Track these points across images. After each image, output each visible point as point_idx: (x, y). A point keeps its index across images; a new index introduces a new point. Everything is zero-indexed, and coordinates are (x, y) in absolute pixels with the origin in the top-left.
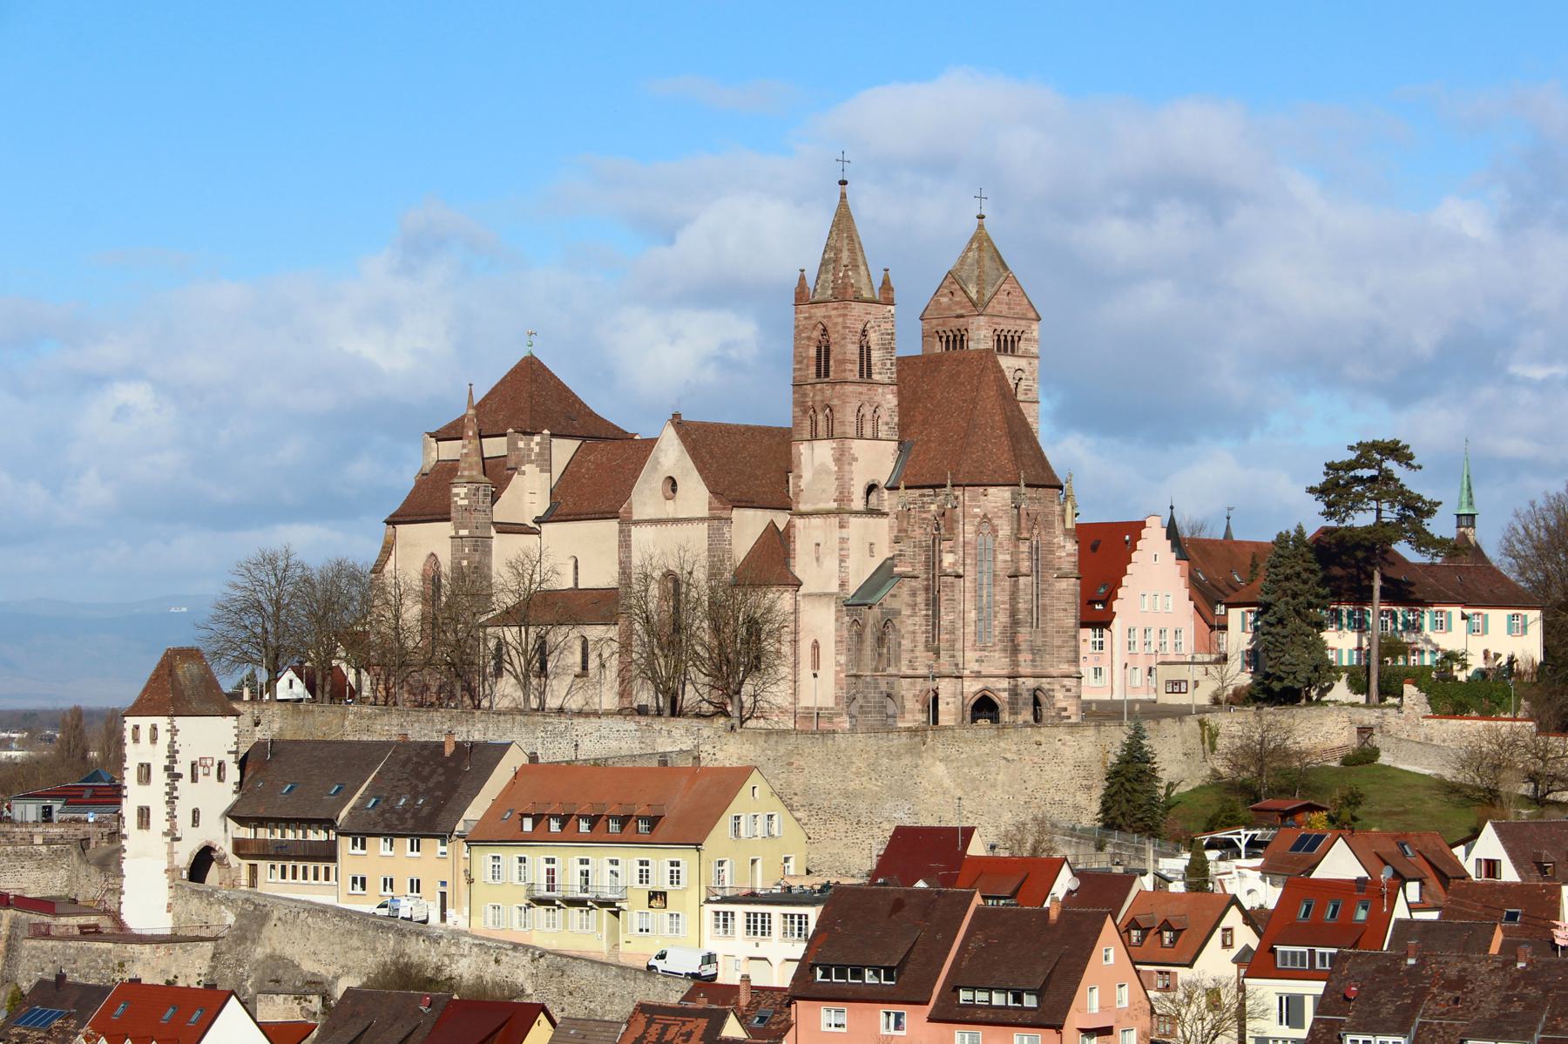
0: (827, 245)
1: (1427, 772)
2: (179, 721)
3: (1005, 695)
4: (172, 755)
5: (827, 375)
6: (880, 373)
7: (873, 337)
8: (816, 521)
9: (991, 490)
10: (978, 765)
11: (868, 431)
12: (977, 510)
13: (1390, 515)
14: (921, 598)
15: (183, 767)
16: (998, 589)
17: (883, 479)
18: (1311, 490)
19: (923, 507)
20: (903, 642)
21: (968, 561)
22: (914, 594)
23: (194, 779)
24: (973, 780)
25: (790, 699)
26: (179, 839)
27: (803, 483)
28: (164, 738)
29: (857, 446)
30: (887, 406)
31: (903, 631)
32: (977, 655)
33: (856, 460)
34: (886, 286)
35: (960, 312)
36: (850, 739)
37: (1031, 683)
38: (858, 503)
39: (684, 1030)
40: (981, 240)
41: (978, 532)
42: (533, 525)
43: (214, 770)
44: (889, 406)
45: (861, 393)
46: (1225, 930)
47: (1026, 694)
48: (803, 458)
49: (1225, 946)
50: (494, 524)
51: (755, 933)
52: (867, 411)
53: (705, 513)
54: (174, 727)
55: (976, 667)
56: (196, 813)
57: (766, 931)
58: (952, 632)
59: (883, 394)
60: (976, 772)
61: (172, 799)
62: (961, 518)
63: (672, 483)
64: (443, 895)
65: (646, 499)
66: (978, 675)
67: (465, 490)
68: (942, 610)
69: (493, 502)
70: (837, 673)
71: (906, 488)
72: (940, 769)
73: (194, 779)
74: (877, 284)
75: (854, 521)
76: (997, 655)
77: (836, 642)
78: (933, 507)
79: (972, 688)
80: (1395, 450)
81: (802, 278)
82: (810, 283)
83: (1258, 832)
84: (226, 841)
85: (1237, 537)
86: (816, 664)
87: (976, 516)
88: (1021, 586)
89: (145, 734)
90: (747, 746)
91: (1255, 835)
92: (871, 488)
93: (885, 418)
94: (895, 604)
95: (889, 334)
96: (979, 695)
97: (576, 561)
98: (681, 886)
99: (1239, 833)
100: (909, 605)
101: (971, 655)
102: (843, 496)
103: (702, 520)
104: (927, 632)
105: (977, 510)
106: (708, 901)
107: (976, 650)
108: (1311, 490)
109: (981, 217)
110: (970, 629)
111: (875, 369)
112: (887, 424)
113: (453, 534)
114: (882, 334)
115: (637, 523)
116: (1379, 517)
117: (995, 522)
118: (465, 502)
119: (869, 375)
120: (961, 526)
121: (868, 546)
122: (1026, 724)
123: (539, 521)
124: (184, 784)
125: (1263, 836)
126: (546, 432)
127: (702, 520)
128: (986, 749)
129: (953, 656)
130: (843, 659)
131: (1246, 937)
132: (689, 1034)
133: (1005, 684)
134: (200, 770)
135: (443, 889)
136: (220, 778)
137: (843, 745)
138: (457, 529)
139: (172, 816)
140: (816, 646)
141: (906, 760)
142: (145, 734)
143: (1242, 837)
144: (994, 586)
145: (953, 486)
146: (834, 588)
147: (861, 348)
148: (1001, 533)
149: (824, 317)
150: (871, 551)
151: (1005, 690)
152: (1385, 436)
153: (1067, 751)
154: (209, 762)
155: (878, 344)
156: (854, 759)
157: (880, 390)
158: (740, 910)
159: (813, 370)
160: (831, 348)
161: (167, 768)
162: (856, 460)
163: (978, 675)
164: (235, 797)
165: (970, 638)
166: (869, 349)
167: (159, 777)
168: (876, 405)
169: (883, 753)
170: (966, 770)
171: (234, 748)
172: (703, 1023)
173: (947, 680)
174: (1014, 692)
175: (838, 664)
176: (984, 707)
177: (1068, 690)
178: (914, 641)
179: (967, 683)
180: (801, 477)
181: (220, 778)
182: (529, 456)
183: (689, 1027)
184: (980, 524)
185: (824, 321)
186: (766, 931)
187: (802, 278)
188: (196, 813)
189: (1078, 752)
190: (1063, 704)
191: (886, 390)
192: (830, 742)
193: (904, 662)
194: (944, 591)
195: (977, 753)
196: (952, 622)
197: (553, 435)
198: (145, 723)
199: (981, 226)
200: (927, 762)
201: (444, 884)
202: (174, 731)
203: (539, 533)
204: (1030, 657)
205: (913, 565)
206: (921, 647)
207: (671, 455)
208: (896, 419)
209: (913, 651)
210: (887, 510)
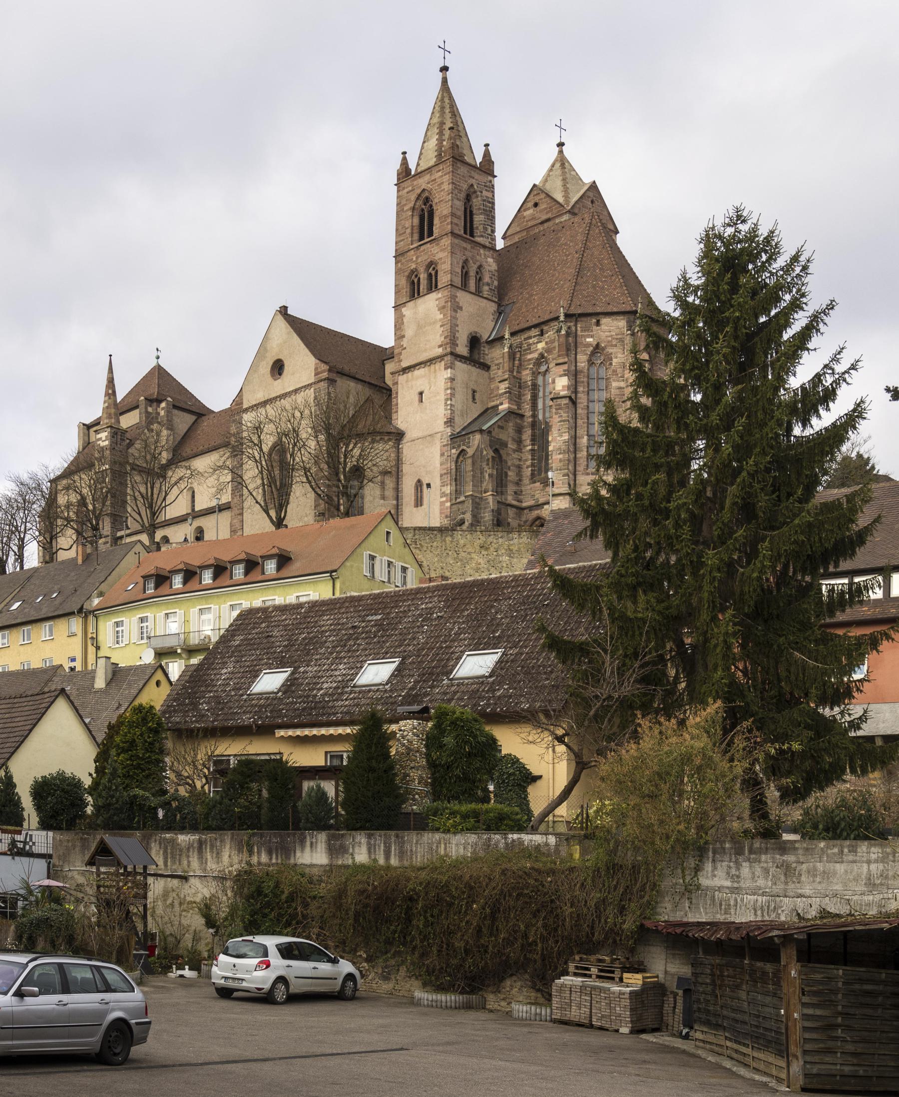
0: (429, 124)
5: (431, 233)
6: (482, 236)
7: (476, 202)
19: (530, 349)
30: (487, 268)
36: (468, 537)
44: (489, 268)
45: (466, 249)
71: (513, 334)
78: (541, 346)
93: (487, 279)
94: (503, 436)
95: (489, 202)
97: (193, 492)
107: (588, 474)
111: (477, 233)
112: (488, 284)
114: (484, 200)
119: (472, 235)
137: (462, 542)
147: (465, 209)
149: (428, 183)
155: (479, 209)
156: (473, 555)
157: (482, 251)
159: (416, 236)
160: (435, 208)
162: (461, 308)
166: (471, 212)
168: (478, 264)
169: (503, 551)
173: (561, 498)
191: (487, 253)
194: (556, 414)
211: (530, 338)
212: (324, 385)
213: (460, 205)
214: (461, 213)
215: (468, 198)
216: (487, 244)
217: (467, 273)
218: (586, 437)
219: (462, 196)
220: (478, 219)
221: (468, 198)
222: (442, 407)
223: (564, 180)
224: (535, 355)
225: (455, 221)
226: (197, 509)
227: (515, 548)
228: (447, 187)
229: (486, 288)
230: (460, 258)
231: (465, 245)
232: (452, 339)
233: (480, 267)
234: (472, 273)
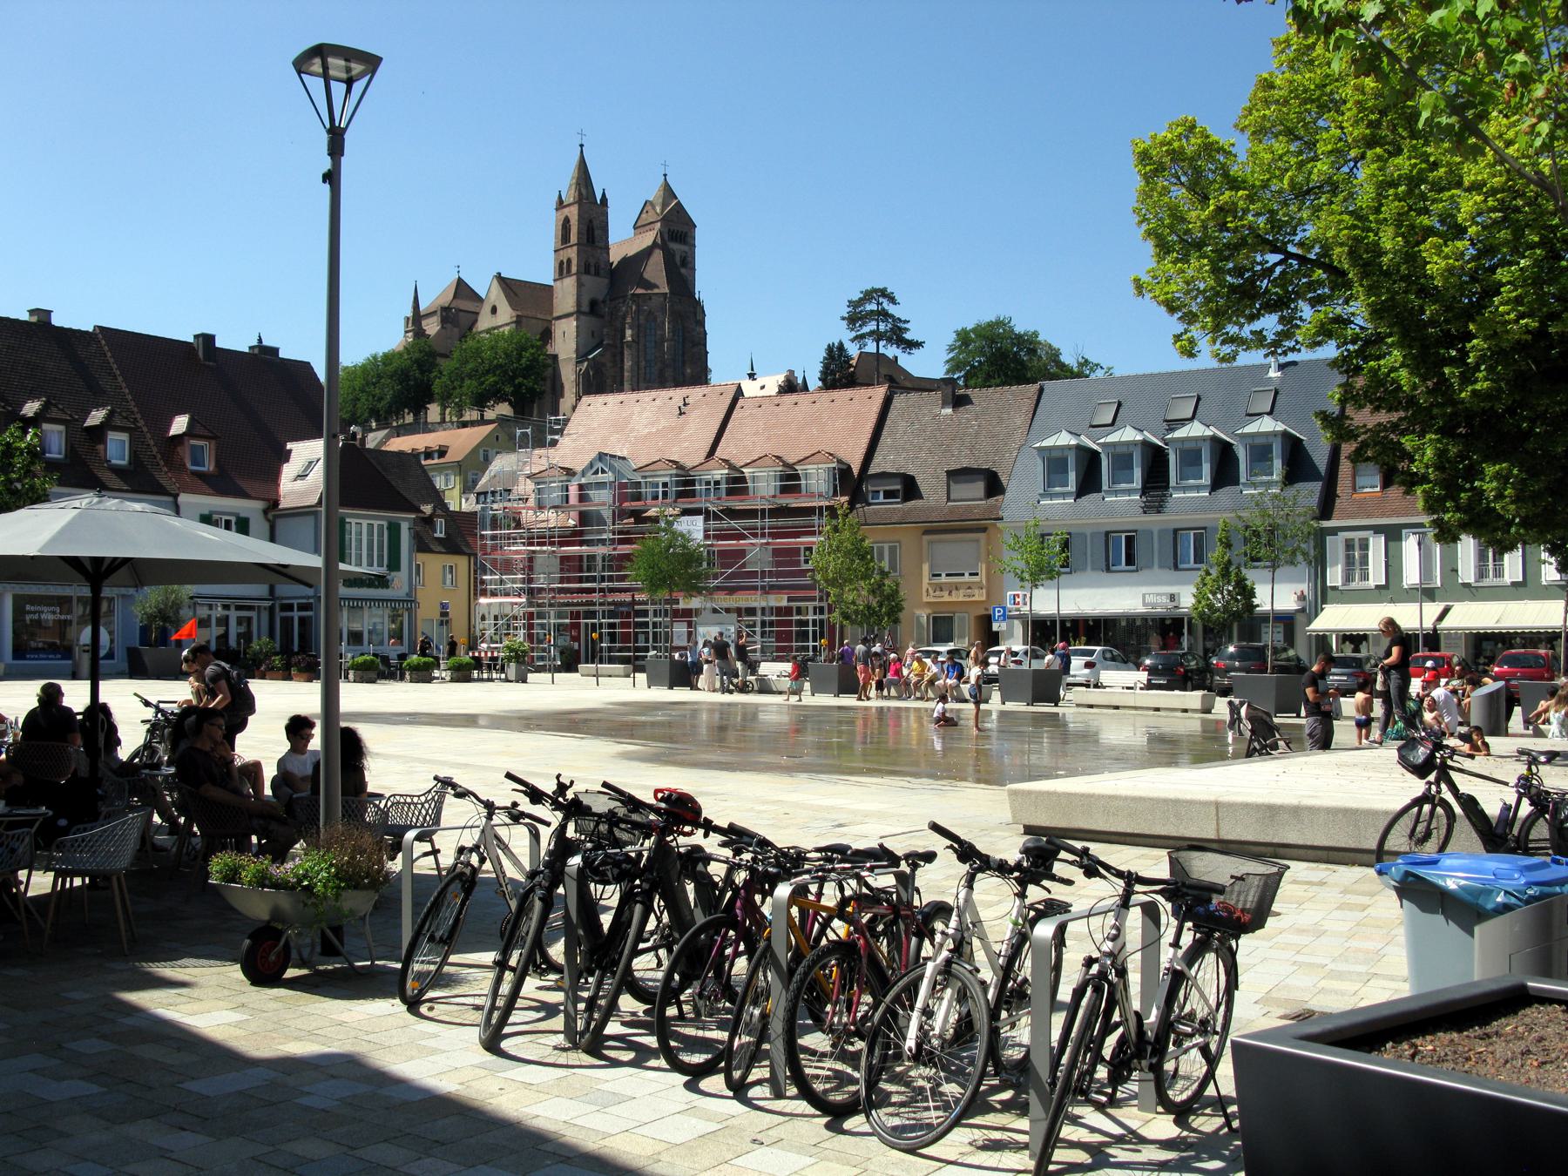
7: (596, 223)
11: (592, 270)
17: (600, 298)
22: (614, 356)
29: (585, 278)
34: (604, 199)
38: (585, 308)
52: (592, 262)
74: (599, 197)
75: (582, 317)
80: (883, 293)
119: (593, 242)
212: (514, 325)
215: (591, 221)
220: (597, 232)
221: (591, 221)
232: (579, 304)
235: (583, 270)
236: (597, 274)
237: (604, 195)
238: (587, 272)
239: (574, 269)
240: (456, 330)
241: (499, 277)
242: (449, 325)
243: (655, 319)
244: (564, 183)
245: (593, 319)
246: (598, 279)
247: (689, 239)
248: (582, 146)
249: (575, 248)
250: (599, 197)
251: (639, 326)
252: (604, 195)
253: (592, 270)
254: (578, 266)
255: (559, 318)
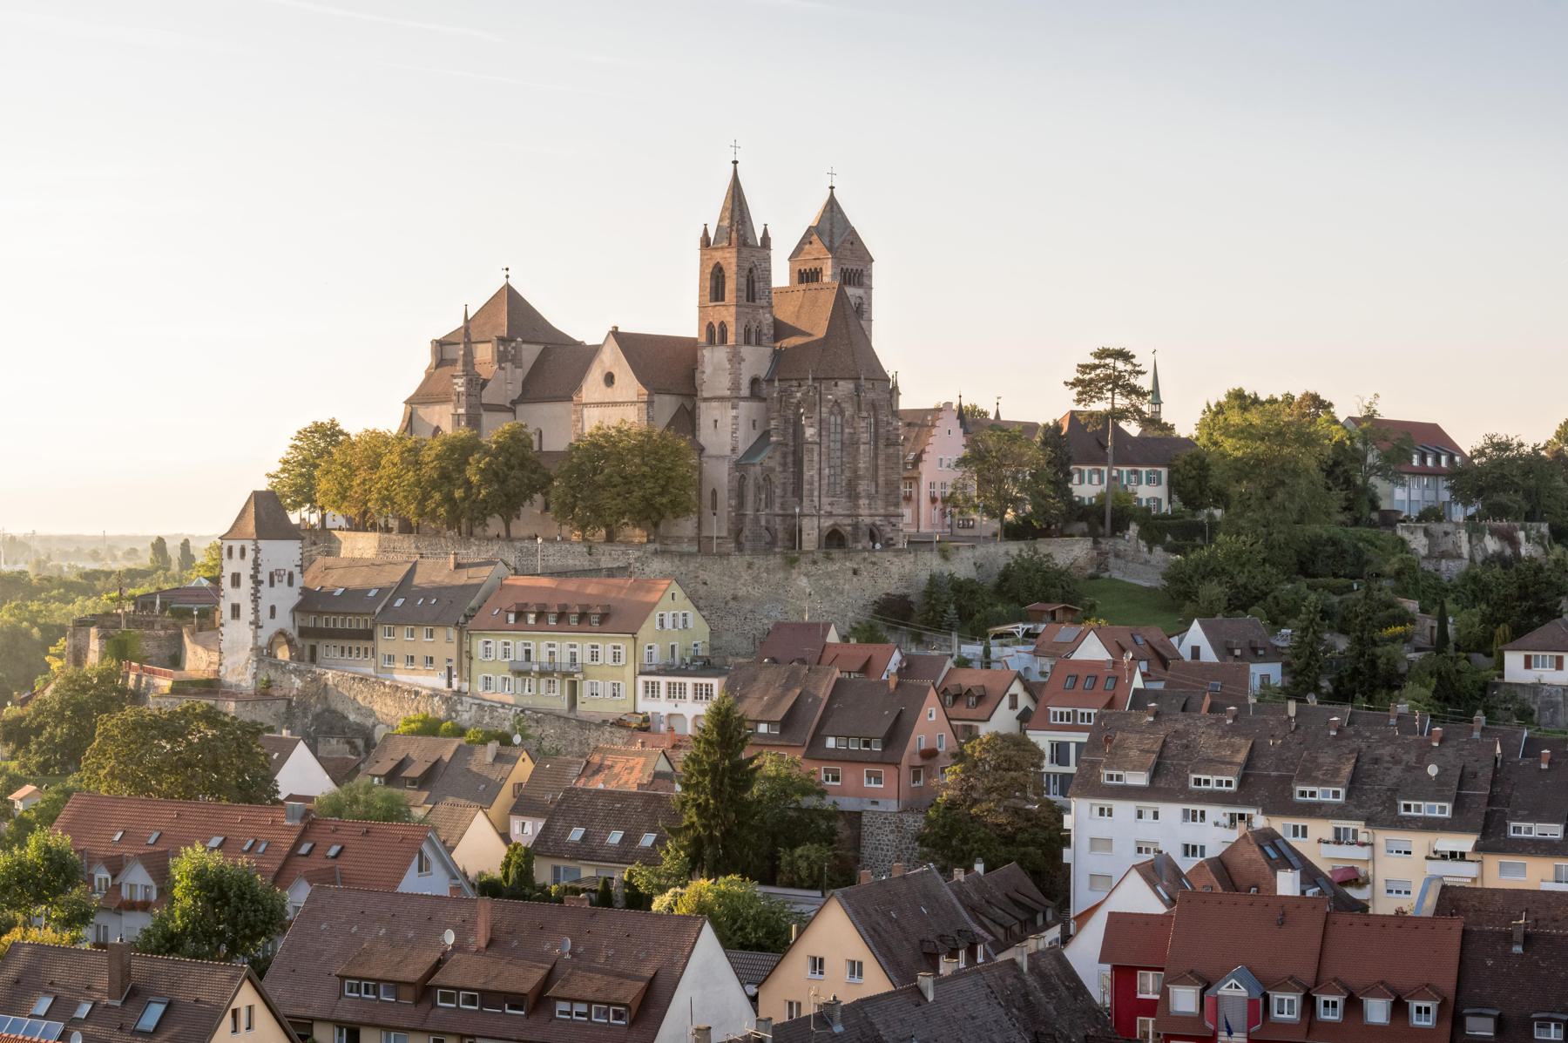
1: (1147, 584)
2: (262, 544)
3: (849, 528)
4: (256, 566)
8: (714, 404)
9: (841, 383)
10: (830, 578)
11: (753, 339)
12: (830, 397)
13: (1121, 402)
14: (790, 459)
15: (264, 576)
16: (844, 453)
17: (763, 375)
18: (1066, 383)
20: (777, 490)
21: (824, 433)
22: (784, 456)
23: (272, 584)
24: (827, 588)
25: (696, 531)
26: (261, 627)
27: (705, 377)
28: (250, 555)
29: (746, 351)
30: (765, 322)
31: (776, 483)
32: (831, 499)
33: (744, 360)
34: (766, 238)
35: (817, 256)
37: (868, 520)
38: (745, 391)
39: (629, 765)
40: (832, 204)
41: (831, 413)
42: (508, 405)
43: (286, 578)
46: (1011, 696)
47: (864, 528)
48: (706, 360)
49: (1011, 708)
50: (482, 405)
51: (675, 697)
52: (754, 326)
53: (635, 399)
54: (257, 547)
55: (828, 508)
56: (273, 609)
57: (683, 696)
58: (812, 484)
59: (764, 314)
60: (829, 583)
61: (256, 598)
62: (818, 402)
63: (609, 379)
64: (449, 669)
65: (592, 387)
66: (830, 514)
67: (462, 380)
68: (805, 468)
69: (482, 389)
70: (729, 512)
72: (803, 582)
73: (272, 584)
74: (759, 235)
75: (742, 404)
76: (844, 500)
77: (729, 490)
78: (799, 395)
79: (827, 523)
81: (706, 230)
82: (712, 235)
83: (1031, 626)
84: (294, 627)
85: (1003, 418)
86: (714, 506)
87: (830, 400)
88: (862, 451)
89: (236, 552)
90: (667, 562)
91: (1028, 629)
92: (755, 382)
93: (765, 331)
96: (830, 529)
98: (621, 664)
99: (1018, 628)
100: (780, 464)
101: (825, 500)
102: (736, 386)
103: (633, 403)
104: (794, 483)
105: (830, 397)
106: (642, 673)
108: (1066, 383)
109: (832, 188)
110: (825, 482)
111: (757, 296)
112: (765, 335)
113: (453, 411)
115: (586, 404)
116: (1113, 404)
117: (843, 405)
118: (462, 389)
119: (754, 300)
120: (818, 408)
121: (751, 423)
122: (864, 549)
123: (514, 402)
124: (264, 588)
125: (1035, 629)
126: (519, 339)
127: (633, 403)
128: (836, 567)
129: (812, 501)
130: (733, 503)
131: (1024, 701)
132: (632, 768)
133: (848, 521)
134: (276, 577)
135: (450, 664)
136: (290, 583)
137: (734, 564)
138: (456, 408)
139: (256, 610)
140: (714, 493)
141: (781, 575)
142: (236, 552)
143: (1020, 630)
144: (842, 450)
145: (814, 379)
146: (727, 451)
147: (748, 280)
148: (847, 413)
150: (754, 425)
151: (849, 525)
152: (1114, 345)
153: (894, 569)
154: (282, 572)
158: (663, 681)
161: (252, 577)
162: (744, 360)
163: (830, 514)
164: (300, 597)
165: (825, 488)
166: (753, 282)
167: (247, 584)
170: (822, 582)
171: (300, 563)
172: (642, 760)
174: (856, 526)
175: (730, 506)
176: (834, 540)
177: (894, 525)
178: (784, 490)
179: (822, 521)
180: (703, 372)
181: (290, 583)
182: (507, 356)
183: (631, 763)
184: (833, 406)
185: (721, 262)
186: (683, 696)
187: (706, 230)
188: (273, 609)
189: (902, 570)
190: (891, 535)
192: (725, 562)
193: (777, 505)
195: (829, 570)
196: (812, 476)
197: (524, 342)
198: (236, 545)
199: (832, 194)
200: (794, 576)
201: (450, 660)
202: (257, 550)
203: (514, 412)
204: (867, 502)
205: (784, 436)
206: (789, 494)
207: (610, 357)
208: (772, 332)
209: (783, 497)
210: (765, 396)
211: (791, 386)
213: (744, 281)
214: (744, 287)
215: (751, 271)
216: (766, 304)
217: (749, 330)
218: (827, 470)
219: (746, 272)
222: (729, 436)
223: (831, 224)
224: (795, 401)
225: (740, 294)
226: (544, 450)
227: (770, 567)
228: (734, 268)
229: (764, 338)
230: (744, 321)
231: (747, 310)
233: (760, 323)
234: (753, 330)
235: (742, 339)
236: (759, 343)
237: (766, 231)
238: (747, 342)
239: (731, 339)
240: (519, 371)
241: (615, 333)
242: (508, 365)
243: (842, 412)
244: (711, 213)
245: (754, 405)
246: (761, 349)
247: (865, 280)
248: (735, 162)
249: (733, 310)
250: (759, 235)
251: (821, 421)
252: (766, 231)
253: (753, 339)
254: (737, 334)
255: (706, 400)
